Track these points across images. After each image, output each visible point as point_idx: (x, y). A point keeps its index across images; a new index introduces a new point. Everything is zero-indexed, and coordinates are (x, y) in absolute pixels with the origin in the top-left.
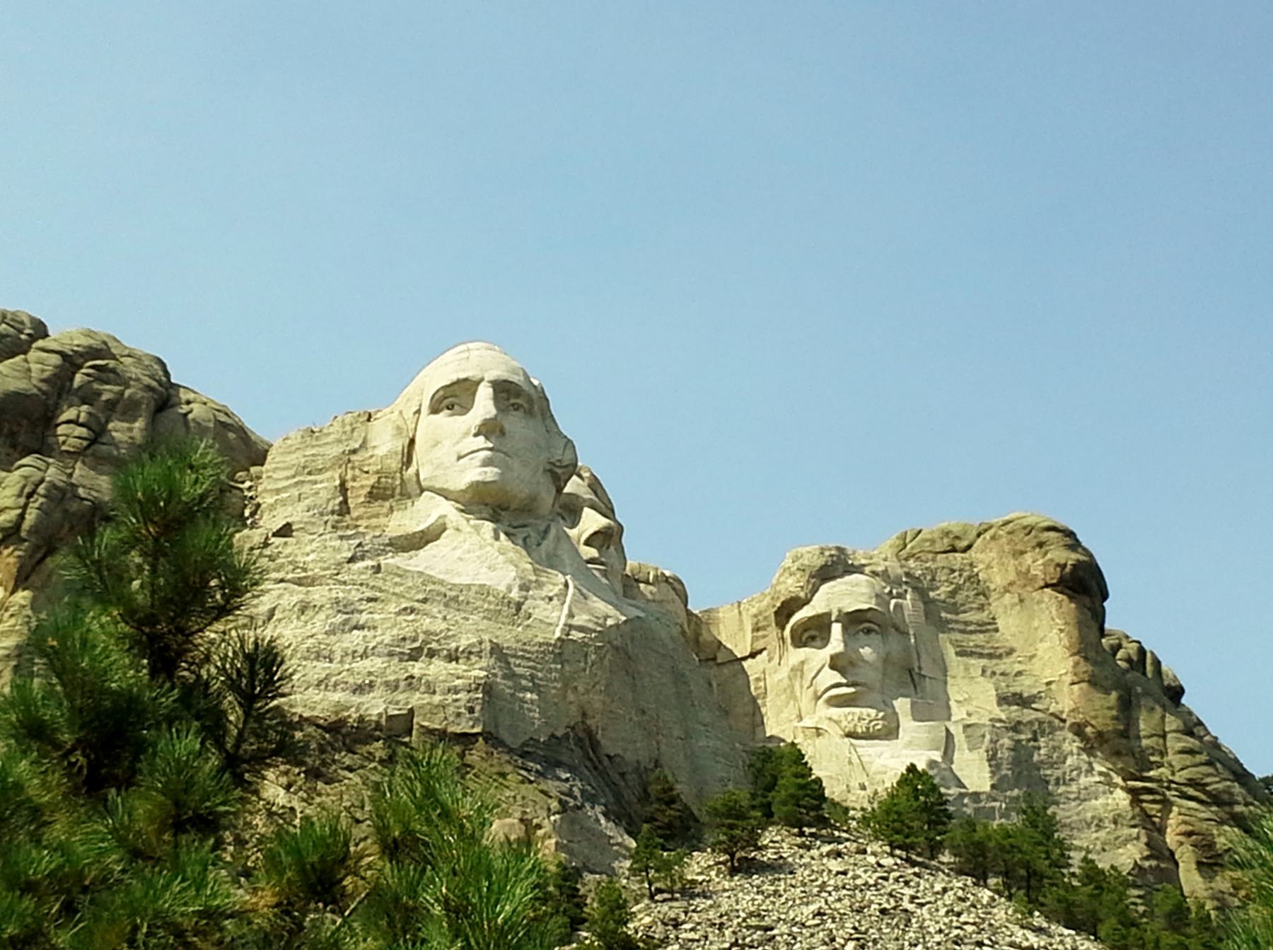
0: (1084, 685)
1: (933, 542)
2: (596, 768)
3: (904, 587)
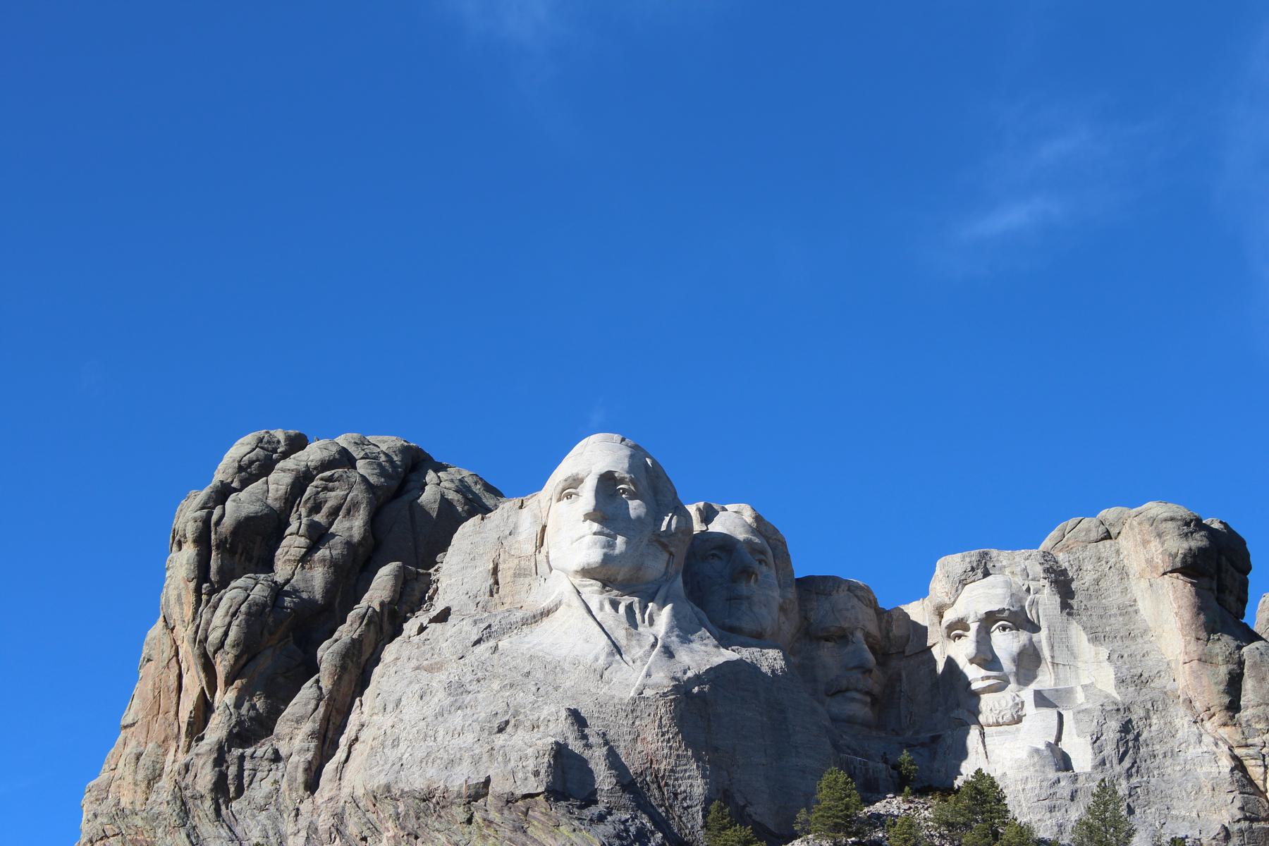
1: (1088, 531)
3: (1043, 582)
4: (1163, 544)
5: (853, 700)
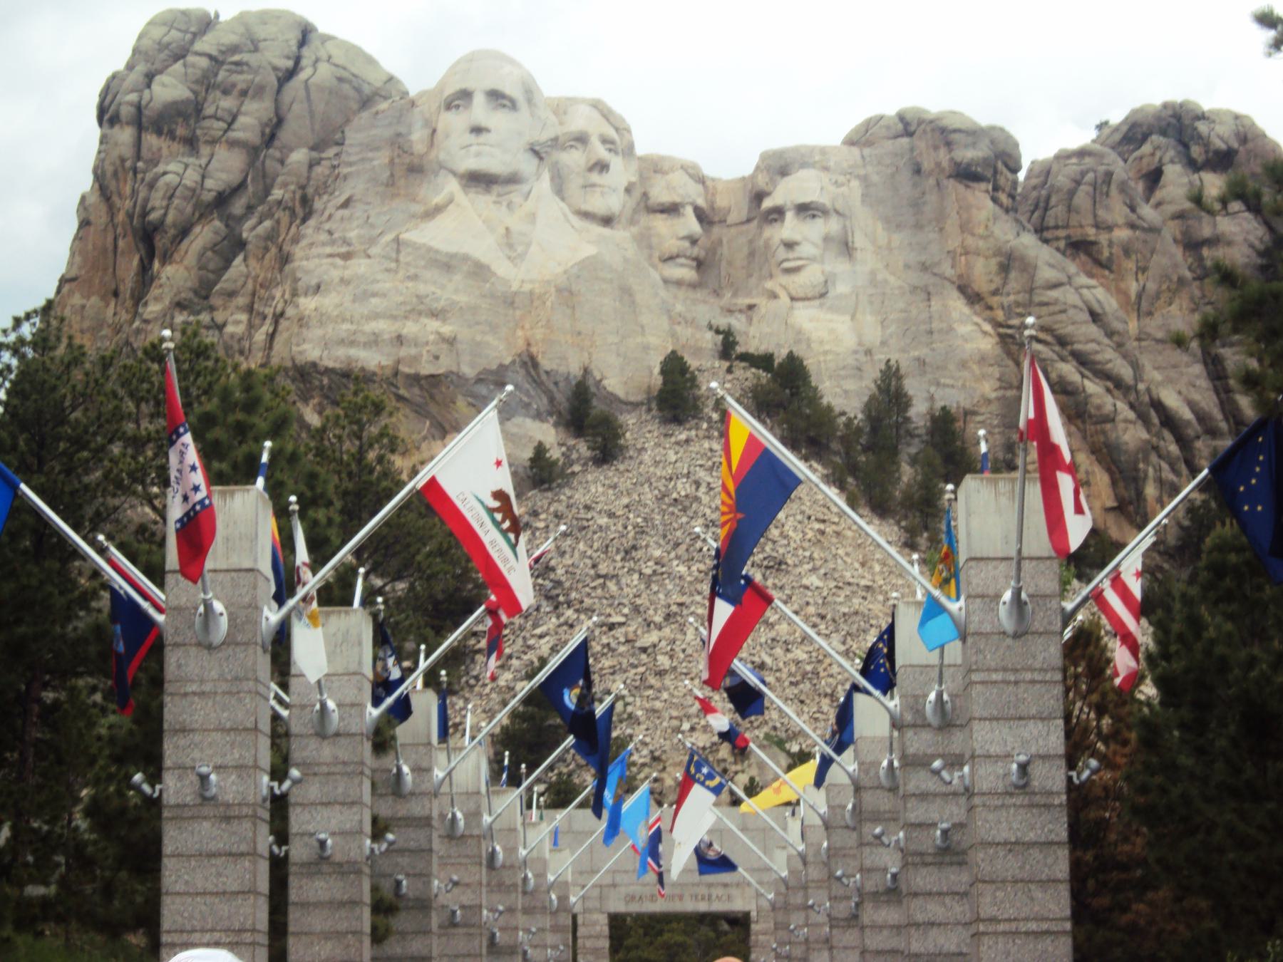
0: (969, 257)
1: (888, 127)
2: (535, 381)
4: (950, 151)
5: (682, 265)
